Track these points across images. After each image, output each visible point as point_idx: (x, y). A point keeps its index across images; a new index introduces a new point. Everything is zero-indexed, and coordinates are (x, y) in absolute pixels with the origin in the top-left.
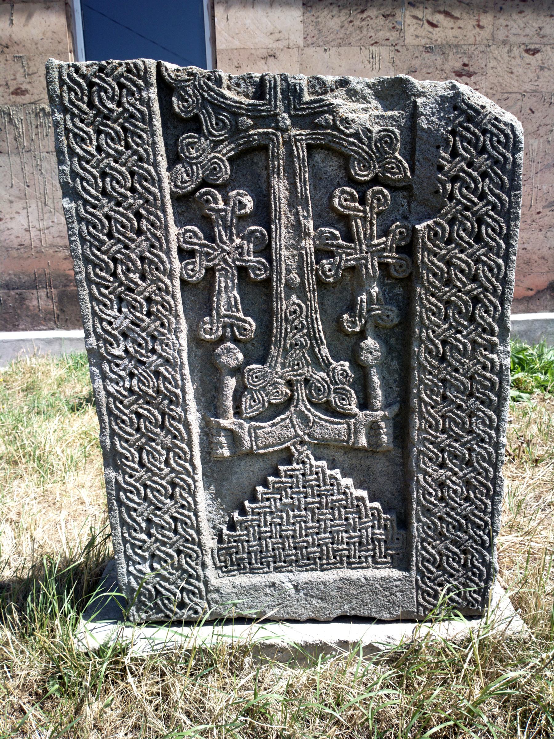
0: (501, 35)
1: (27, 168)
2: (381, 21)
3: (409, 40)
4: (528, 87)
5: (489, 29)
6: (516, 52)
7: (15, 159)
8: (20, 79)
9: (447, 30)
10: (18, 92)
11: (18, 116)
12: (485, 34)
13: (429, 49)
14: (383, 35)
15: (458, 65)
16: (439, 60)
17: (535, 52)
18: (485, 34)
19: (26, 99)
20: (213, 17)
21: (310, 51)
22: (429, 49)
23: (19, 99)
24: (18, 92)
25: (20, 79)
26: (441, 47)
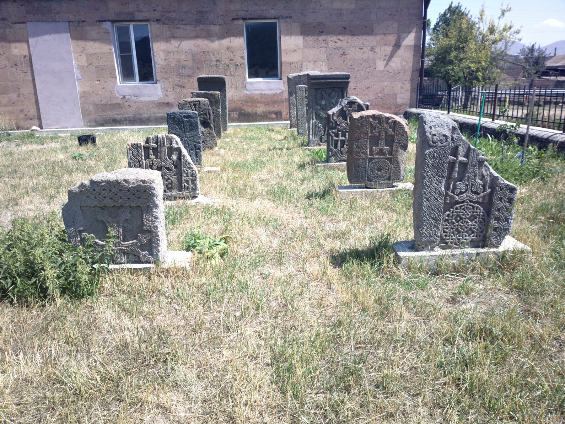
0: (353, 44)
1: (233, 80)
2: (322, 42)
3: (330, 46)
4: (360, 58)
5: (350, 43)
6: (357, 49)
7: (229, 77)
8: (232, 56)
9: (339, 44)
10: (231, 60)
11: (231, 66)
12: (349, 44)
13: (335, 49)
14: (323, 45)
15: (342, 52)
16: (337, 51)
17: (362, 49)
18: (349, 44)
19: (233, 62)
20: (280, 39)
21: (305, 49)
22: (335, 49)
23: (231, 62)
24: (231, 60)
25: (232, 56)
26: (338, 48)
